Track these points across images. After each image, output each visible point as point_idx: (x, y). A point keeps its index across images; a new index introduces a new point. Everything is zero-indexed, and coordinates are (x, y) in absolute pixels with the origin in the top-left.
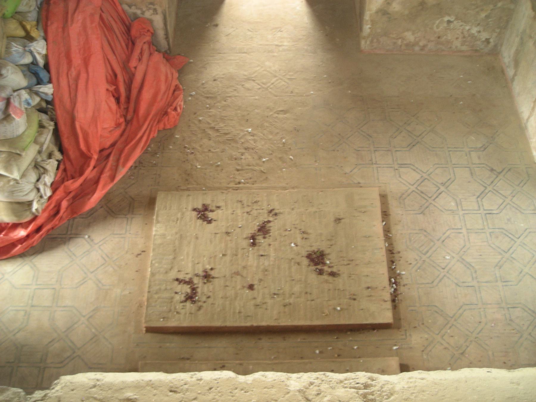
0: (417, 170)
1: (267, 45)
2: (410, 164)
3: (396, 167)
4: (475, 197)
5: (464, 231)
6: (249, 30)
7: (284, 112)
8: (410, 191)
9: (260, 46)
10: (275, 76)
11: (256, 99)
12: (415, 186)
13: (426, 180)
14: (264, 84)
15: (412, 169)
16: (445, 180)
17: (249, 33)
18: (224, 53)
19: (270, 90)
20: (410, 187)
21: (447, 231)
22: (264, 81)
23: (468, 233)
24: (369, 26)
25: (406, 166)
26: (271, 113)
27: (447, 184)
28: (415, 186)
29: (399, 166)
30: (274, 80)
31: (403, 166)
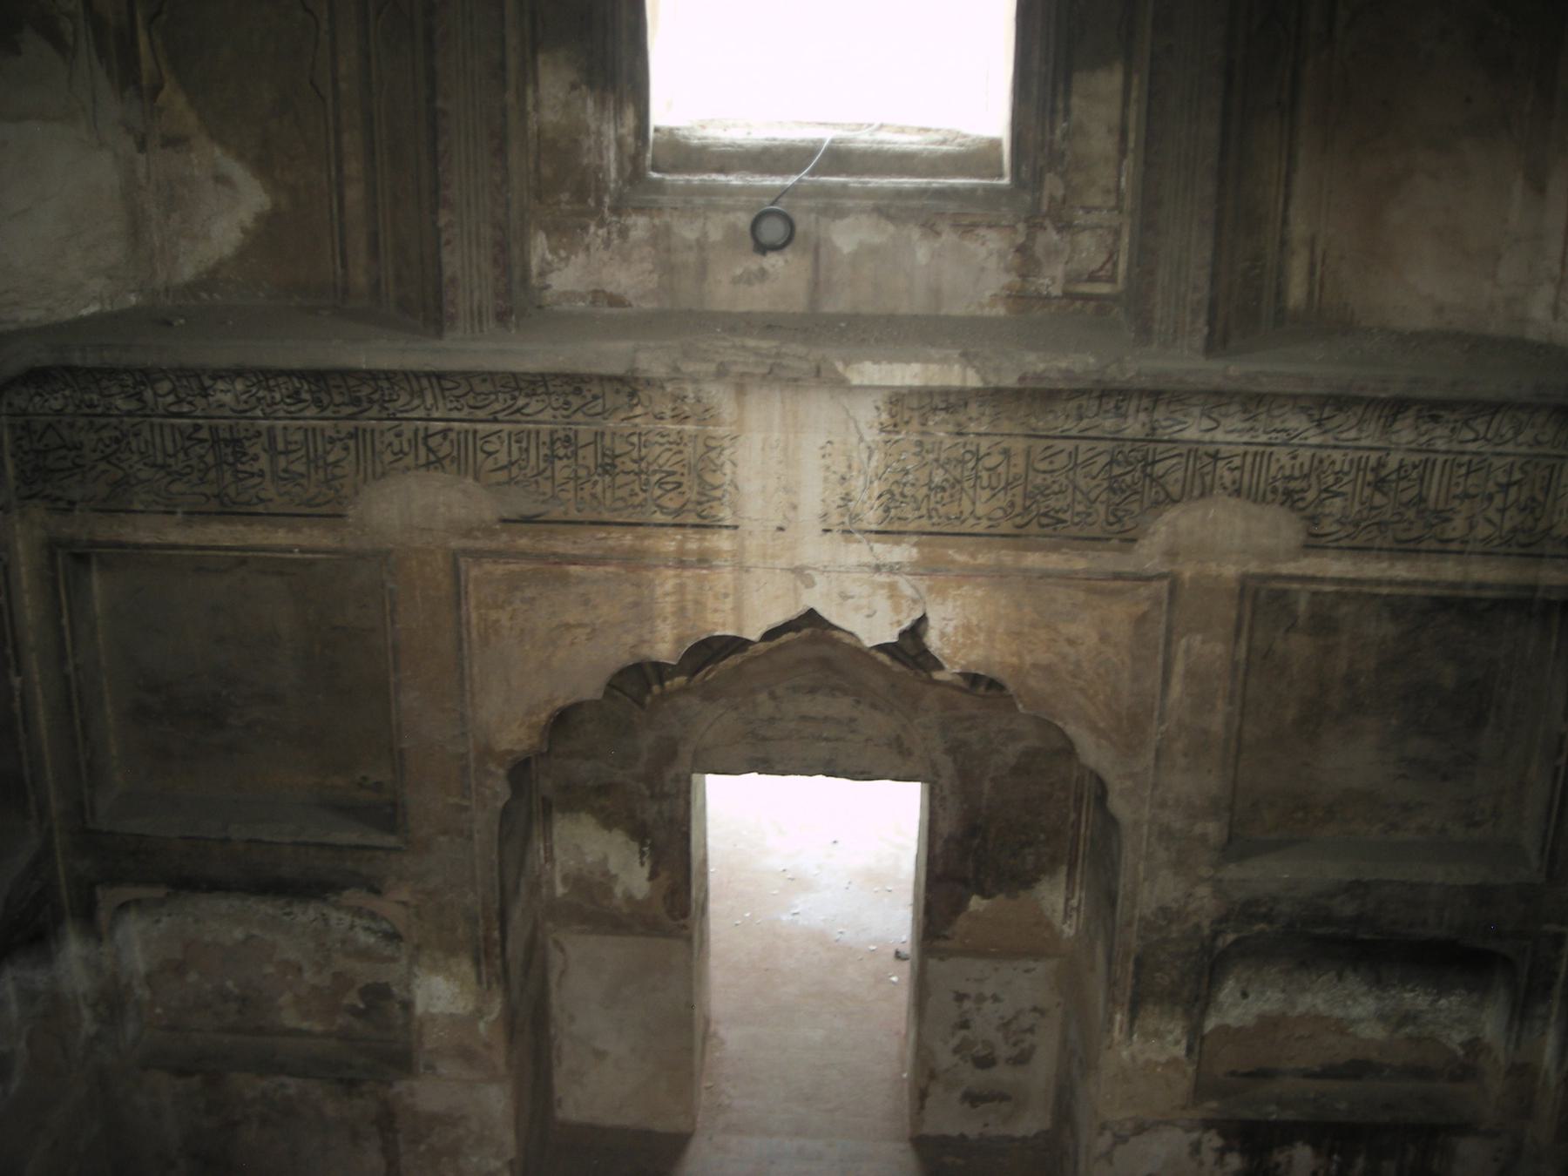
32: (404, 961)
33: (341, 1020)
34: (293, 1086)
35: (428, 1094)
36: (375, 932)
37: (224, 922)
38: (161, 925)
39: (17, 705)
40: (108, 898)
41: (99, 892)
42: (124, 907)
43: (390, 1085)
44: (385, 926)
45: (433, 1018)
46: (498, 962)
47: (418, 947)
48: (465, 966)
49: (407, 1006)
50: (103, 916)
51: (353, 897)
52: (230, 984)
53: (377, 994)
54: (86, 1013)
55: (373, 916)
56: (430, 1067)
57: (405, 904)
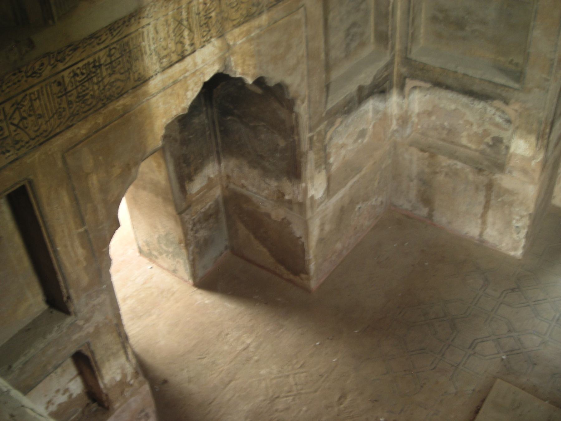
1: (236, 357)
6: (199, 359)
7: (343, 397)
9: (232, 364)
10: (288, 376)
11: (306, 411)
14: (290, 392)
17: (204, 361)
18: (215, 399)
19: (303, 391)
22: (286, 389)
24: (313, 263)
26: (336, 409)
30: (291, 379)
32: (511, 131)
33: (482, 147)
34: (460, 165)
35: (506, 181)
36: (503, 118)
37: (449, 101)
38: (426, 97)
39: (390, 8)
40: (410, 83)
41: (407, 81)
42: (415, 88)
43: (494, 174)
44: (506, 117)
45: (516, 155)
46: (546, 141)
47: (517, 128)
48: (533, 139)
49: (508, 148)
50: (407, 89)
51: (498, 103)
52: (446, 124)
53: (498, 141)
54: (394, 122)
55: (503, 112)
56: (510, 172)
57: (516, 111)
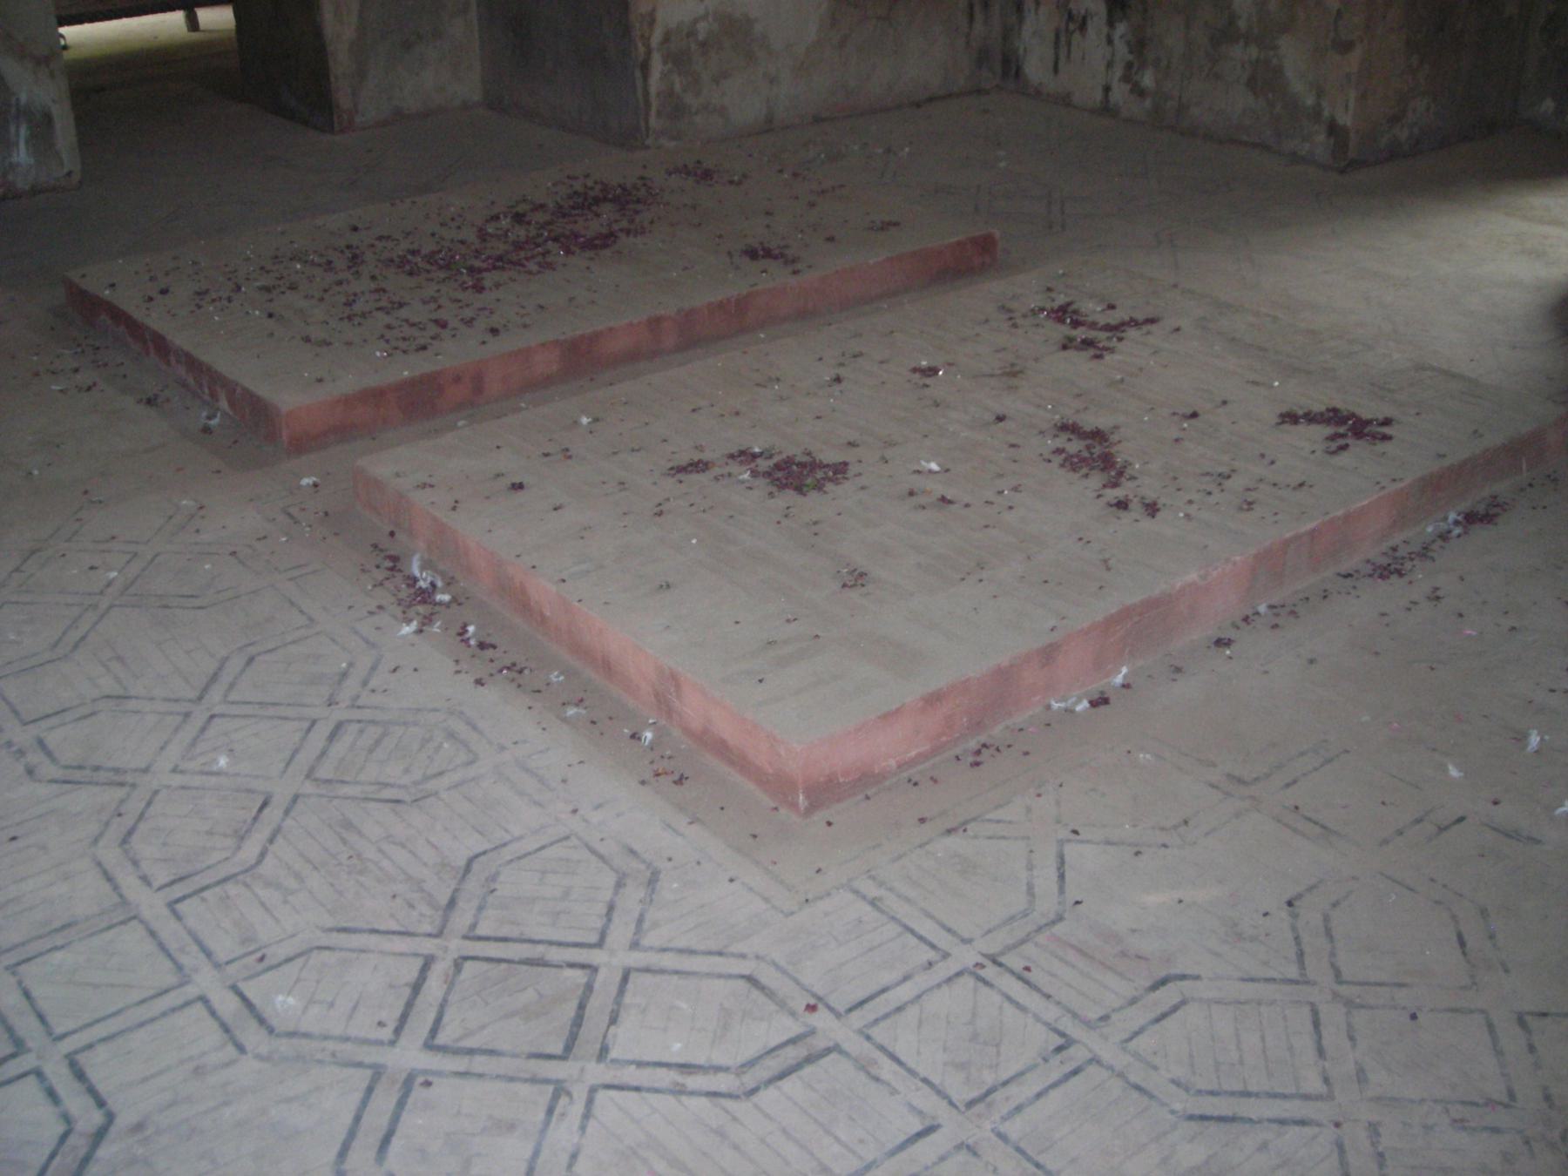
0: (666, 1077)
2: (754, 1091)
3: (821, 1019)
4: (124, 1119)
5: (151, 905)
8: (620, 933)
12: (606, 981)
13: (557, 1048)
15: (718, 1069)
16: (412, 1121)
20: (636, 959)
21: (263, 854)
23: (124, 901)
25: (773, 1065)
27: (384, 1102)
28: (606, 981)
29: (819, 1043)
31: (792, 1054)
